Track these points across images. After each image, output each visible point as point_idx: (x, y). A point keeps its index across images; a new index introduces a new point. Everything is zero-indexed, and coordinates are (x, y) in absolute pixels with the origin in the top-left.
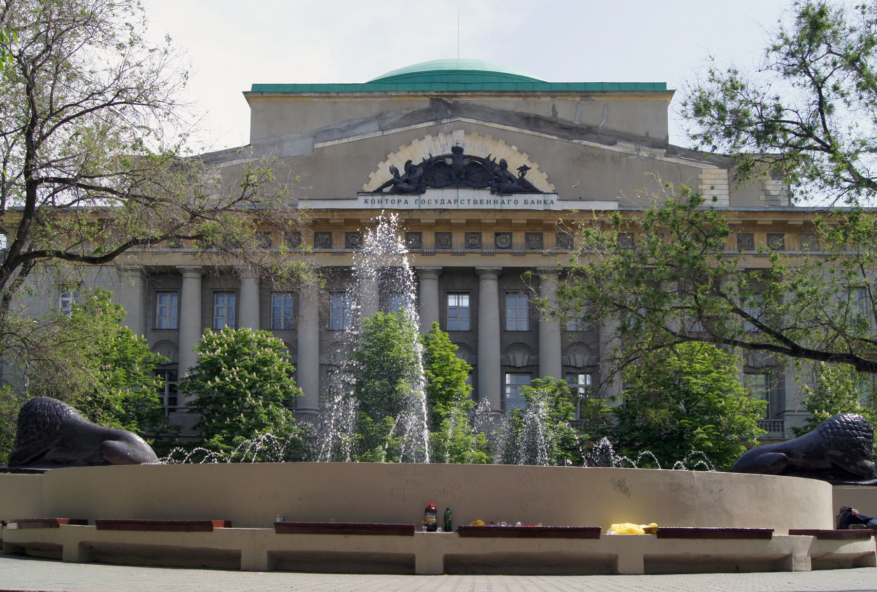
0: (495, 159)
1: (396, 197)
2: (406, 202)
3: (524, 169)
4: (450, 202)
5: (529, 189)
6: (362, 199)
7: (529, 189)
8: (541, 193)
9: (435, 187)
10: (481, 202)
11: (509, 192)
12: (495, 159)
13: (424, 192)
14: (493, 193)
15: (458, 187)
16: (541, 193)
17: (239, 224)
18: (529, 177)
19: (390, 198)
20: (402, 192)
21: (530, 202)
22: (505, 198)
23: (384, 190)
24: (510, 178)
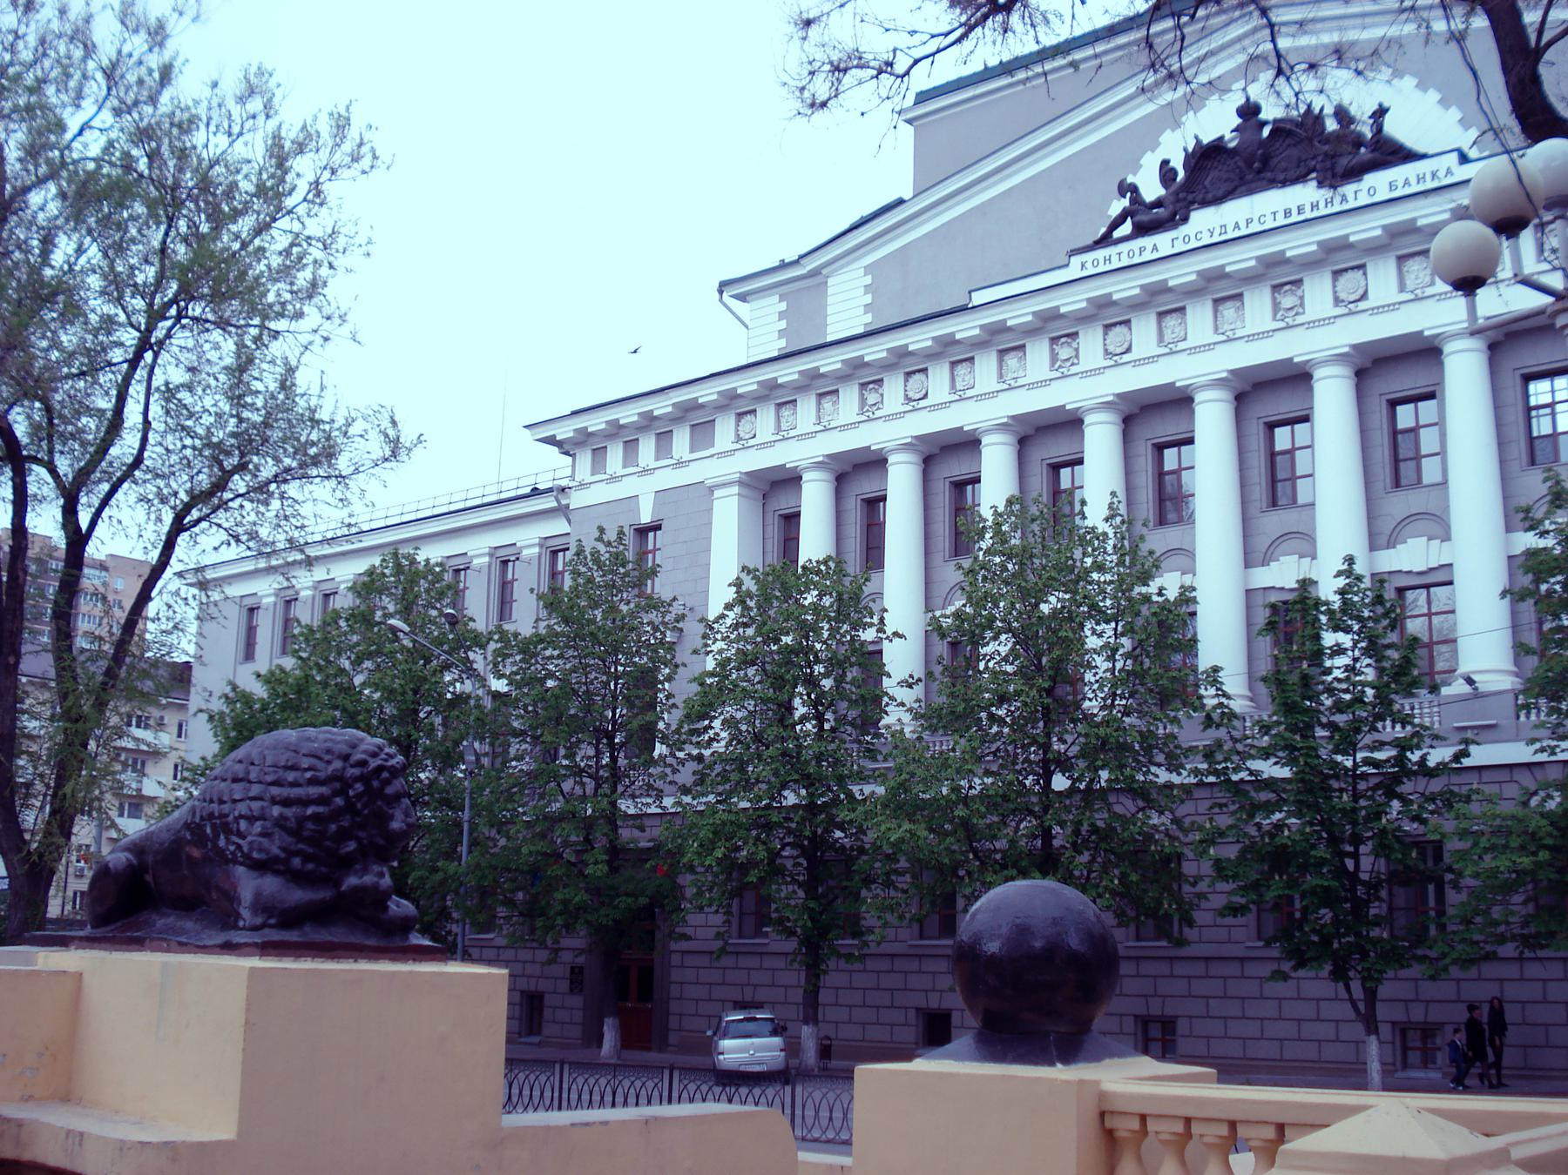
0: (1322, 109)
1: (1147, 241)
2: (1155, 248)
3: (1381, 112)
4: (1237, 226)
5: (1391, 153)
6: (1076, 261)
7: (1391, 153)
8: (1424, 156)
9: (1205, 203)
10: (1287, 213)
11: (1356, 173)
12: (1322, 109)
13: (1185, 220)
14: (1321, 185)
15: (1251, 192)
16: (1424, 156)
17: (550, 466)
18: (1394, 128)
19: (1124, 247)
20: (1141, 230)
21: (1400, 184)
22: (1349, 189)
23: (1117, 234)
24: (1358, 141)
